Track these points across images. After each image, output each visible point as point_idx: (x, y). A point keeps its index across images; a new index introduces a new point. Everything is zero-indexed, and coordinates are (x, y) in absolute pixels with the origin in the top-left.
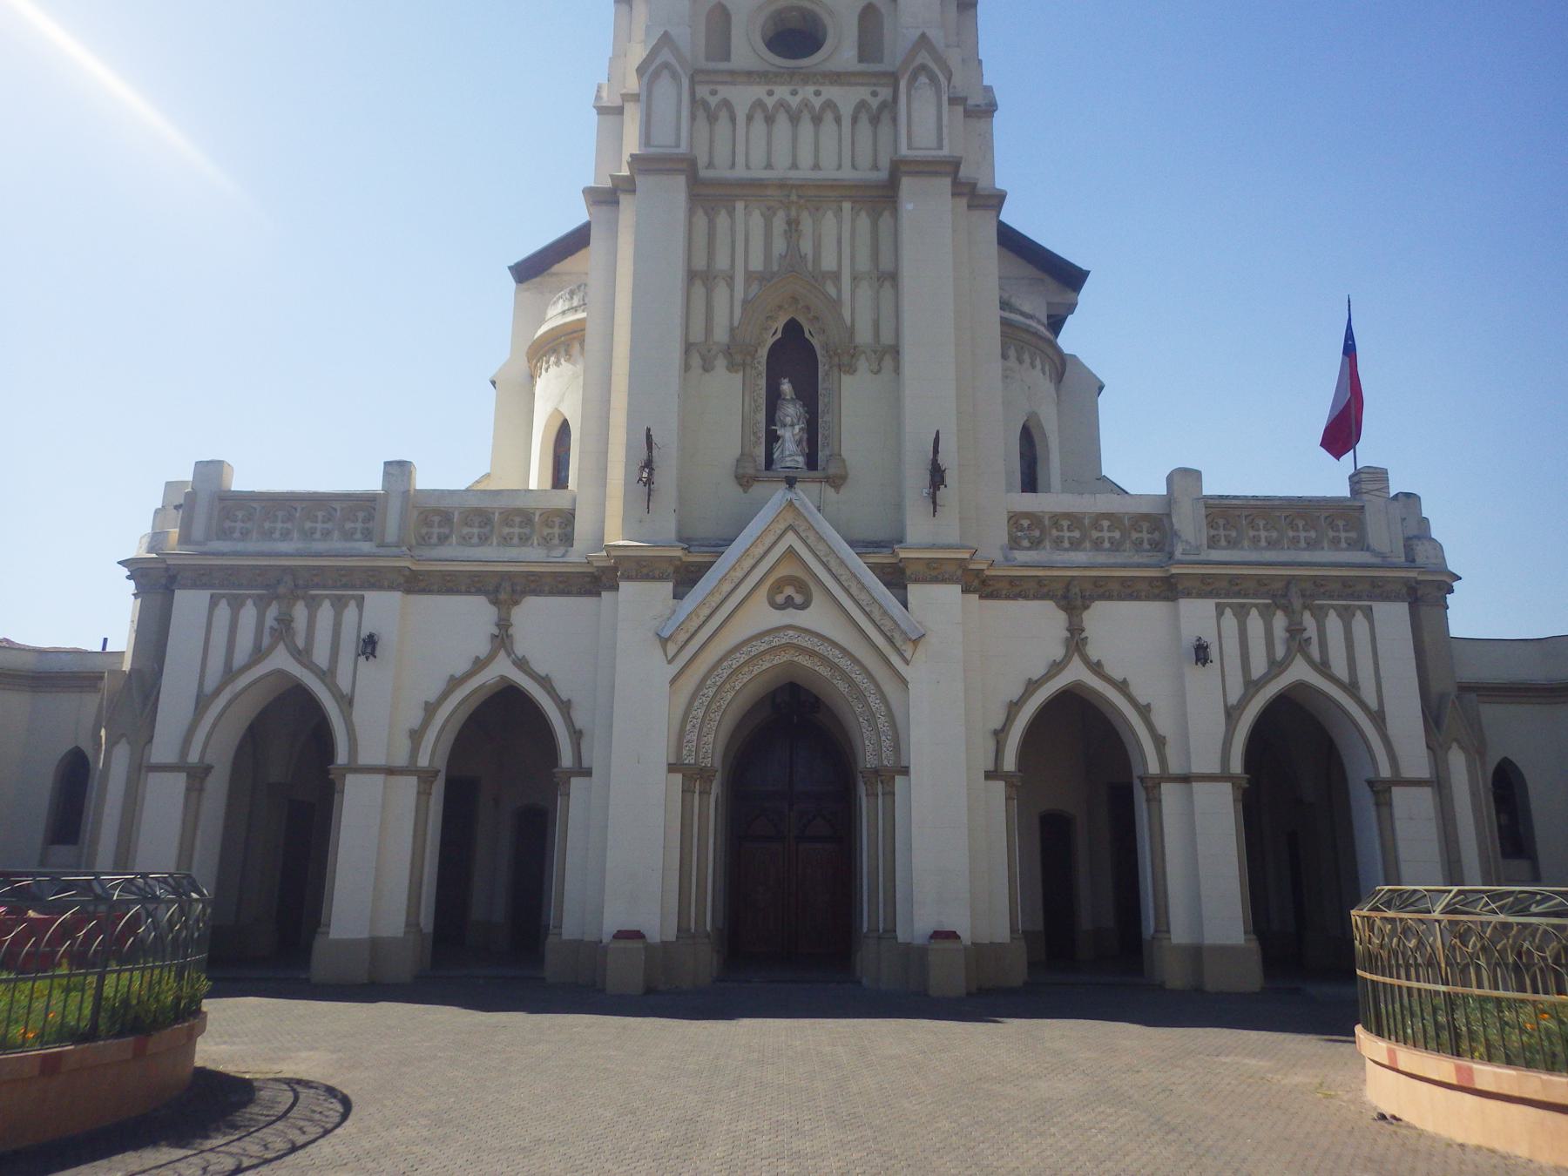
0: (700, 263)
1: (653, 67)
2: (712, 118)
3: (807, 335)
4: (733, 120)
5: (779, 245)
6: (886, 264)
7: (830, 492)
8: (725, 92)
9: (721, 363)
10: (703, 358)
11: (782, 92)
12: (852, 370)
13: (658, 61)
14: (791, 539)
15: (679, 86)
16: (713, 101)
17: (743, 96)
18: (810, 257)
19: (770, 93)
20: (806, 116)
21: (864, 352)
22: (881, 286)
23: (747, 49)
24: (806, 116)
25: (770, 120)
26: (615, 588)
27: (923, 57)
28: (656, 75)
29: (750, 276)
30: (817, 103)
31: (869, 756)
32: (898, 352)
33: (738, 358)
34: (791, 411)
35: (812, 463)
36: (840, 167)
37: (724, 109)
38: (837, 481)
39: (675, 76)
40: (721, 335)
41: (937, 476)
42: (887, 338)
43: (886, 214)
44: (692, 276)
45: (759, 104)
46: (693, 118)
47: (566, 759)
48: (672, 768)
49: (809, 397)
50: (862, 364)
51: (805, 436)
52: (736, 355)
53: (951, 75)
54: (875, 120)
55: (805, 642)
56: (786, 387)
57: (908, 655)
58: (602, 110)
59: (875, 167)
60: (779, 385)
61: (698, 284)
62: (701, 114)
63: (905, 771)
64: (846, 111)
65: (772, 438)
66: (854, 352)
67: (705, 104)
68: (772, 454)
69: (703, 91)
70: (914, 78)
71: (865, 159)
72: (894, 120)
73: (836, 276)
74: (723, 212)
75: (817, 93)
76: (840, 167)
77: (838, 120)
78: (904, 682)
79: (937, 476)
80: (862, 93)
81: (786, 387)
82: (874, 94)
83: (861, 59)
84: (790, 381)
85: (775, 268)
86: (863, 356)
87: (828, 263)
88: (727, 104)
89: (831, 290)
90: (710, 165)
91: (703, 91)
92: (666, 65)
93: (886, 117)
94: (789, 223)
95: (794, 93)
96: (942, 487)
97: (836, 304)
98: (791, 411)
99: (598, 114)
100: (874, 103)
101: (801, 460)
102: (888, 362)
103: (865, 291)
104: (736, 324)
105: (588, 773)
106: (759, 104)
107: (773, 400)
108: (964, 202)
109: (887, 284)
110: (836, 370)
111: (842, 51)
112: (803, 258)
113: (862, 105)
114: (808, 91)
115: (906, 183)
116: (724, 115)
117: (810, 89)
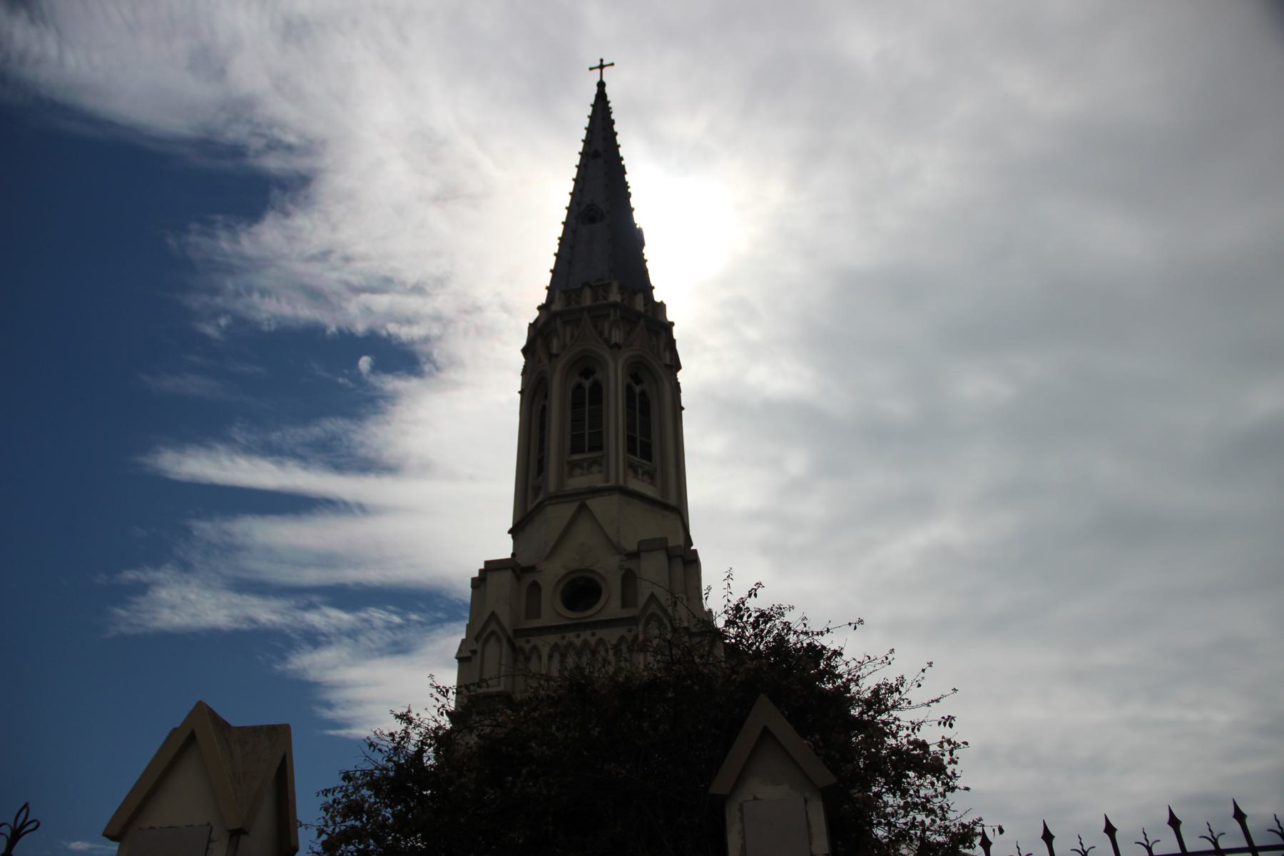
1: (484, 636)
4: (540, 658)
8: (535, 641)
11: (571, 636)
13: (488, 631)
16: (527, 647)
23: (552, 610)
27: (653, 608)
28: (487, 640)
30: (593, 641)
39: (499, 640)
67: (522, 650)
69: (520, 642)
75: (593, 634)
82: (630, 631)
88: (535, 648)
91: (520, 642)
92: (493, 633)
95: (578, 636)
99: (459, 662)
106: (556, 646)
111: (611, 605)
114: (586, 635)
117: (589, 633)
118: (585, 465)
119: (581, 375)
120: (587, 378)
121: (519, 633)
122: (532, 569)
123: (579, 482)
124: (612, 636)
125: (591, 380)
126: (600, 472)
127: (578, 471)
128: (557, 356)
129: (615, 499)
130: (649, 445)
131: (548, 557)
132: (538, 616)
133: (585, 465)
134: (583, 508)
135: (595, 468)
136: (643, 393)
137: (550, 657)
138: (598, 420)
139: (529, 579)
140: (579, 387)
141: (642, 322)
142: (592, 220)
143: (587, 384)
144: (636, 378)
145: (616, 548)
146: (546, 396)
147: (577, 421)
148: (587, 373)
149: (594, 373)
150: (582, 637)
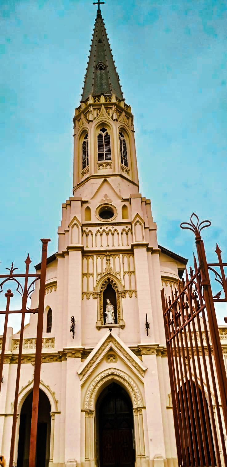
0: (85, 272)
2: (87, 235)
3: (113, 287)
5: (105, 266)
6: (132, 270)
7: (121, 329)
8: (90, 228)
9: (91, 297)
10: (87, 296)
11: (104, 228)
12: (123, 297)
14: (111, 345)
15: (79, 229)
16: (87, 231)
17: (94, 229)
18: (113, 268)
19: (101, 228)
20: (110, 234)
21: (128, 292)
22: (131, 275)
23: (95, 219)
24: (110, 234)
25: (101, 235)
26: (66, 359)
28: (73, 227)
29: (98, 274)
30: (113, 230)
31: (136, 404)
32: (136, 291)
33: (96, 296)
34: (110, 308)
35: (116, 322)
36: (119, 245)
37: (90, 233)
38: (122, 327)
40: (91, 290)
41: (147, 326)
42: (133, 288)
43: (131, 256)
44: (83, 275)
45: (98, 231)
46: (82, 235)
47: (53, 410)
48: (82, 411)
49: (114, 304)
50: (127, 295)
51: (114, 314)
52: (95, 294)
53: (145, 222)
54: (127, 234)
55: (116, 372)
56: (108, 301)
57: (143, 374)
58: (59, 234)
59: (128, 245)
60: (106, 301)
61: (85, 277)
62: (84, 234)
63: (145, 408)
64: (120, 232)
65: (105, 315)
66: (125, 292)
67: (85, 231)
68: (106, 320)
70: (136, 224)
71: (125, 243)
72: (132, 233)
73: (119, 273)
74: (91, 258)
75: (113, 228)
76: (119, 245)
77: (118, 234)
78: (142, 383)
79: (147, 326)
80: (124, 227)
81: (108, 301)
83: (123, 218)
84: (109, 300)
85: (104, 271)
86: (127, 294)
87: (117, 270)
88: (90, 231)
89: (118, 276)
90: (87, 247)
91: (84, 229)
93: (130, 233)
94: (107, 260)
96: (149, 328)
97: (119, 280)
98: (110, 308)
100: (127, 229)
101: (113, 321)
102: (134, 294)
103: (127, 276)
104: (95, 286)
105: (59, 413)
107: (105, 304)
108: (150, 253)
109: (132, 274)
110: (120, 297)
111: (118, 217)
112: (111, 269)
113: (124, 230)
114: (110, 227)
115: (136, 250)
116: (90, 234)
118: (105, 165)
119: (101, 130)
120: (104, 132)
121: (83, 225)
122: (87, 202)
123: (103, 171)
124: (120, 228)
125: (105, 133)
126: (111, 168)
127: (101, 167)
128: (92, 121)
129: (119, 178)
130: (127, 160)
131: (92, 198)
132: (90, 220)
133: (105, 165)
134: (105, 180)
135: (108, 167)
136: (124, 141)
137: (96, 235)
138: (108, 148)
139: (86, 205)
140: (100, 135)
141: (124, 111)
142: (101, 69)
143: (104, 134)
144: (121, 135)
145: (119, 197)
146: (86, 138)
147: (100, 149)
148: (103, 130)
149: (106, 130)
150: (108, 229)
